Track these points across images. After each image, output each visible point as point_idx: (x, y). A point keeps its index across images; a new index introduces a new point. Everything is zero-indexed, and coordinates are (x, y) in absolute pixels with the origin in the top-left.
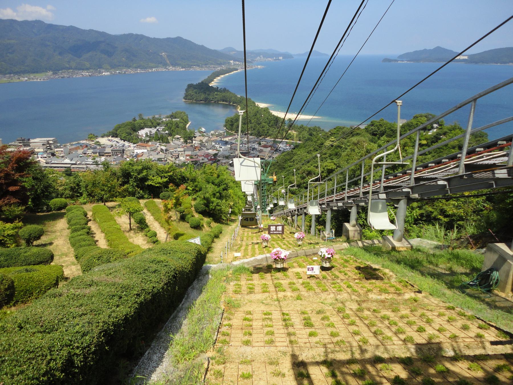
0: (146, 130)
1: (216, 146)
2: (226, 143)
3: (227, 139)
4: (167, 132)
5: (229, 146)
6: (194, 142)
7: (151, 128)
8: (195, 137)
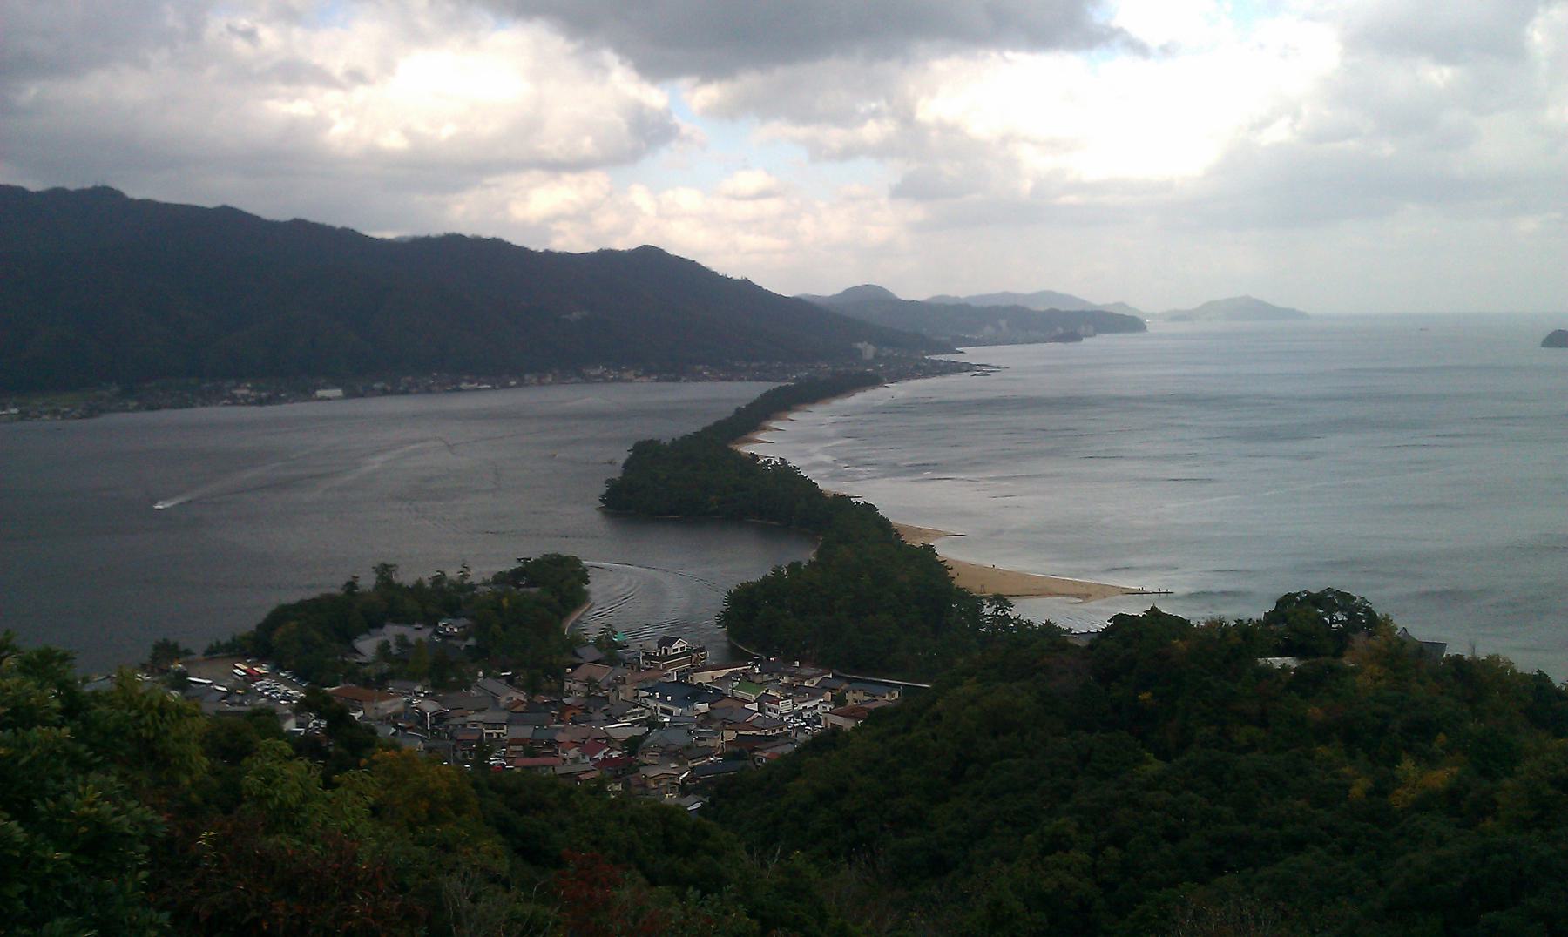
0: (391, 632)
1: (652, 704)
2: (699, 693)
3: (704, 678)
4: (471, 641)
5: (704, 707)
6: (567, 685)
7: (410, 622)
8: (575, 667)
